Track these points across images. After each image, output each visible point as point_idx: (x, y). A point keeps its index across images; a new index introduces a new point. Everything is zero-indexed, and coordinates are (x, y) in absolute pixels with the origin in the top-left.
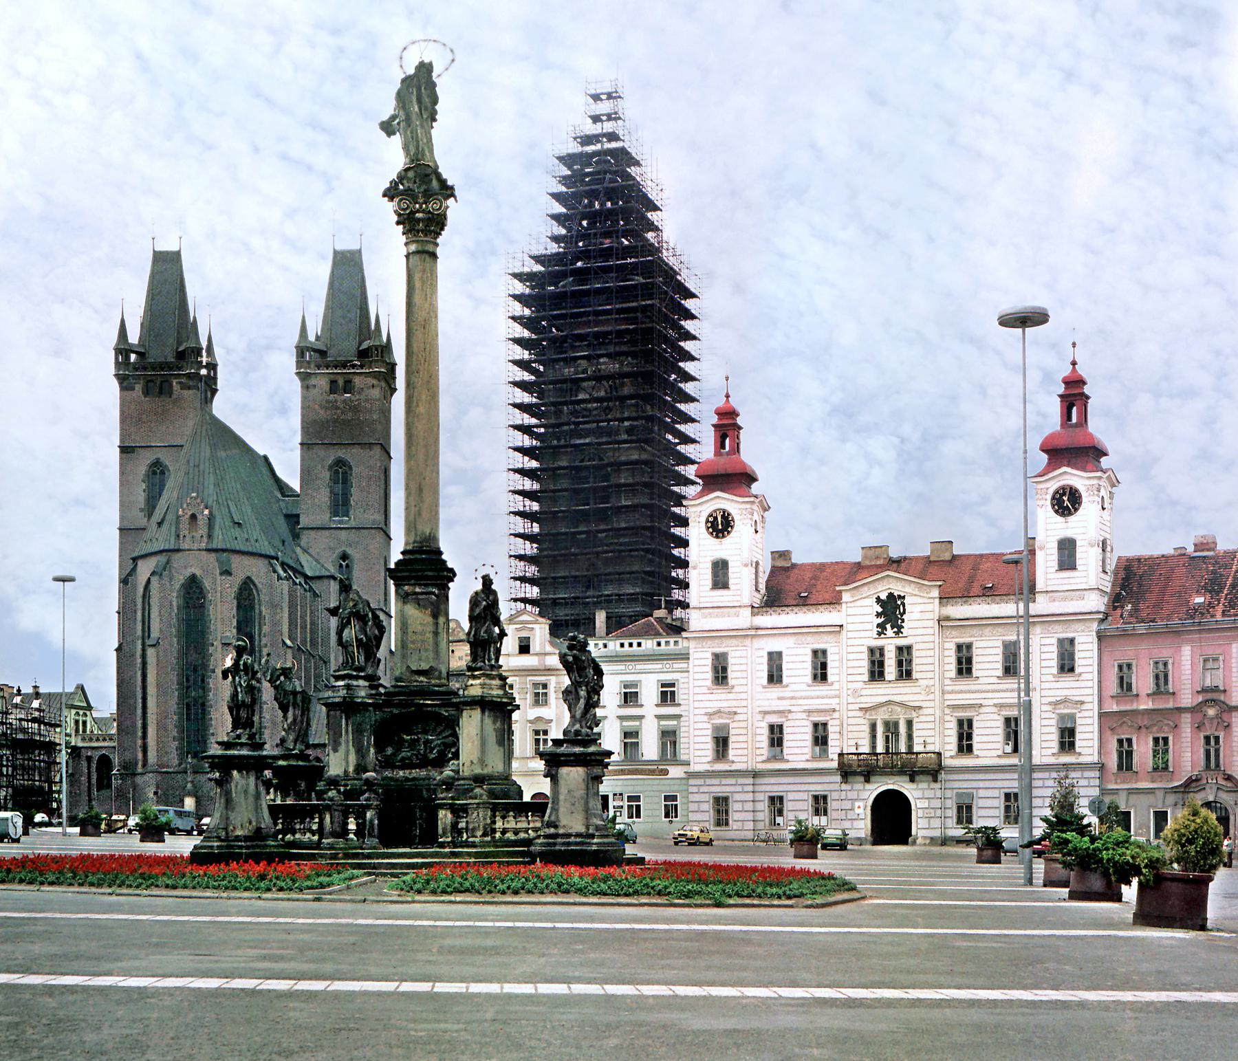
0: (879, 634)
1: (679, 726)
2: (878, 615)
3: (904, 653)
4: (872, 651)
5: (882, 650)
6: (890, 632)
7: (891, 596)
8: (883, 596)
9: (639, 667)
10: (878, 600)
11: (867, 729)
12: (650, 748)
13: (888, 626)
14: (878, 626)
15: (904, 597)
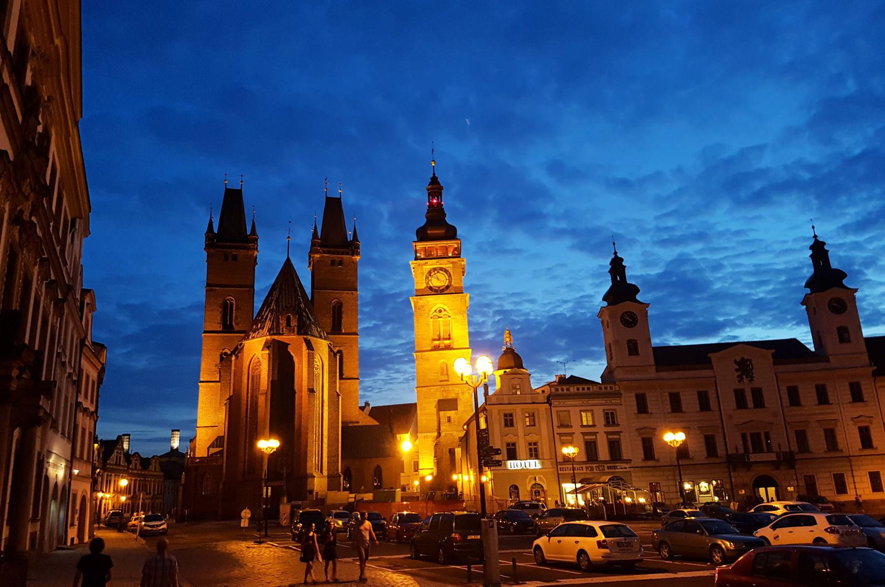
0: (739, 381)
1: (620, 438)
2: (737, 370)
3: (757, 394)
4: (736, 391)
5: (743, 390)
6: (746, 380)
7: (743, 359)
8: (738, 360)
9: (590, 402)
10: (735, 362)
11: (740, 438)
12: (604, 453)
13: (744, 377)
14: (738, 377)
15: (751, 360)
